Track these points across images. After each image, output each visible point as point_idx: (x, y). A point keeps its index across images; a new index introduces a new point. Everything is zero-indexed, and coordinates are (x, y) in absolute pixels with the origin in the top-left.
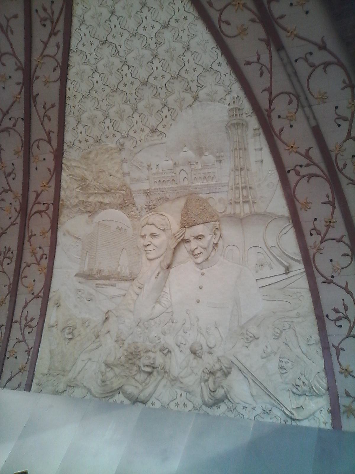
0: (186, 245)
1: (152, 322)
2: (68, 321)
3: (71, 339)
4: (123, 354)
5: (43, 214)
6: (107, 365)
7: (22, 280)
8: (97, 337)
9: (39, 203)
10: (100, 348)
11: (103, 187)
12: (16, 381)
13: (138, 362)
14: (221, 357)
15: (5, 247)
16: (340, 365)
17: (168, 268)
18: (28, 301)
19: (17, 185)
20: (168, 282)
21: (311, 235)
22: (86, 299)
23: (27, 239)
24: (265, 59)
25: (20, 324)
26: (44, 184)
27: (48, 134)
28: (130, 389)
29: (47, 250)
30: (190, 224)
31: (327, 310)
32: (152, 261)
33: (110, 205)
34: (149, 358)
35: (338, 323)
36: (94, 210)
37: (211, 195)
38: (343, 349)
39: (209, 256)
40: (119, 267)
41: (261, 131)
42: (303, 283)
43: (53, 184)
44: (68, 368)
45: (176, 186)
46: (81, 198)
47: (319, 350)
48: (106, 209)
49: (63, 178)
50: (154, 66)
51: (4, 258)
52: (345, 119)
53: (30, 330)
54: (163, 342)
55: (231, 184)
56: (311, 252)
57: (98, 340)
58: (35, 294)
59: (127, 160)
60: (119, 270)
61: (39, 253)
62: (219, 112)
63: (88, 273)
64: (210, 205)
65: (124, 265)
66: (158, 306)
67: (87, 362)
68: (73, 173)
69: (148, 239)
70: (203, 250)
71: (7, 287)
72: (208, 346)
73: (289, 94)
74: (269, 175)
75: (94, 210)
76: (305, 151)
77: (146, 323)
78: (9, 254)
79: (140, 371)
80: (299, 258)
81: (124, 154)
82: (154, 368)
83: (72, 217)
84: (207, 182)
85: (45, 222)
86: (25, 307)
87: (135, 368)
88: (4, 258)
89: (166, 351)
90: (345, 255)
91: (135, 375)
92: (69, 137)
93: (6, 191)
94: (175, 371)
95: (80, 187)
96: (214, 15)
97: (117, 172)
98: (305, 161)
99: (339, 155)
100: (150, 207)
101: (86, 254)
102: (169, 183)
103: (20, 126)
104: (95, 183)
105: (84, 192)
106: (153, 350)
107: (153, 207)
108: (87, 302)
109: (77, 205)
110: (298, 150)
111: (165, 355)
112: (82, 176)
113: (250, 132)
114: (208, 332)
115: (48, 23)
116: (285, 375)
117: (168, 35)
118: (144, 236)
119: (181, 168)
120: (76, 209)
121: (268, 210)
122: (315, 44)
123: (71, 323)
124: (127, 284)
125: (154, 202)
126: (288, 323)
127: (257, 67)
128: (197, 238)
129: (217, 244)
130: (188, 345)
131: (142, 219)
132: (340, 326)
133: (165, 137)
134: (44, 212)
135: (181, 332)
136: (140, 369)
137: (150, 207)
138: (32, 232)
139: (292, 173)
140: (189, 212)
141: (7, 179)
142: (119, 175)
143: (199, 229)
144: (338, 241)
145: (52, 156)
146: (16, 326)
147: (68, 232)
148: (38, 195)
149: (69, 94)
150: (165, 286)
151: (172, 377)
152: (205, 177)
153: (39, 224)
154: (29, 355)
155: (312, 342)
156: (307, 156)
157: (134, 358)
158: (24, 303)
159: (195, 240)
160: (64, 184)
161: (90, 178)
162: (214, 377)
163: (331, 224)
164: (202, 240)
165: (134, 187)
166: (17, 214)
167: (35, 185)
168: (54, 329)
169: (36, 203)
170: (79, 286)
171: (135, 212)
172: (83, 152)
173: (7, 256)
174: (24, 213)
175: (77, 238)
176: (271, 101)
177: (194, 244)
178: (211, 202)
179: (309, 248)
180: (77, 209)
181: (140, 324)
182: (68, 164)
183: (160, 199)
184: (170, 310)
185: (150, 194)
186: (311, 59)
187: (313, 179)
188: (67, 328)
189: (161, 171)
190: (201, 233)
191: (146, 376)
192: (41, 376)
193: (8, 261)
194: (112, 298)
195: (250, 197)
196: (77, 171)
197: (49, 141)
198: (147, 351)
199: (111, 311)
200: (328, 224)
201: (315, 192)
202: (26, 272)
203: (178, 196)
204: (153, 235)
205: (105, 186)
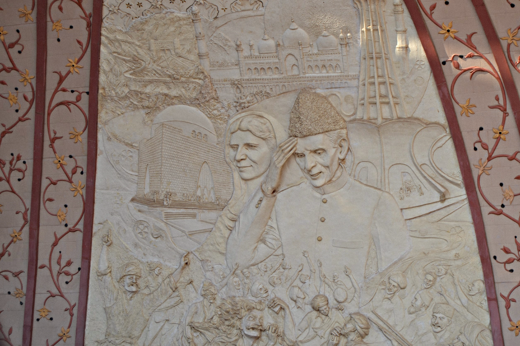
0: (298, 159)
1: (254, 269)
2: (127, 265)
3: (134, 292)
4: (216, 313)
5: (72, 106)
7: (44, 204)
9: (64, 90)
10: (181, 306)
11: (168, 73)
13: (238, 323)
14: (356, 314)
15: (12, 154)
16: (510, 320)
17: (274, 192)
18: (58, 236)
19: (27, 62)
20: (273, 213)
21: (475, 149)
22: (152, 235)
25: (50, 270)
26: (71, 62)
29: (83, 162)
30: (305, 133)
31: (494, 250)
32: (249, 182)
33: (180, 99)
34: (255, 318)
35: (509, 267)
36: (155, 105)
37: (334, 91)
38: (514, 301)
39: (334, 176)
40: (199, 189)
41: (404, 6)
44: (136, 333)
45: (281, 76)
46: (133, 88)
47: (483, 302)
48: (173, 104)
49: (102, 56)
51: (11, 170)
53: (68, 278)
54: (272, 296)
55: (361, 78)
56: (475, 172)
57: (177, 293)
58: (69, 226)
59: (204, 36)
60: (199, 193)
61: (70, 165)
63: (152, 197)
64: (332, 106)
66: (262, 246)
67: (164, 325)
68: (119, 50)
69: (242, 152)
70: (323, 168)
71: (20, 215)
72: (336, 300)
74: (417, 67)
75: (155, 105)
76: (466, 37)
77: (245, 270)
78: (20, 165)
79: (242, 335)
80: (459, 179)
81: (200, 27)
82: (261, 330)
83: (120, 113)
84: (328, 72)
86: (55, 244)
88: (11, 170)
89: (277, 307)
91: (237, 340)
93: (8, 70)
94: (291, 335)
95: (130, 70)
97: (189, 52)
99: (512, 47)
100: (243, 105)
101: (146, 168)
102: (269, 73)
104: (155, 66)
105: (138, 79)
106: (258, 308)
107: (246, 105)
108: (154, 239)
109: (126, 97)
110: (456, 35)
111: (277, 313)
112: (135, 56)
114: (336, 281)
116: (439, 335)
118: (235, 147)
119: (290, 51)
120: (127, 102)
121: (415, 115)
123: (132, 269)
124: (212, 215)
125: (248, 98)
126: (444, 267)
128: (315, 152)
129: (343, 160)
130: (308, 300)
131: (231, 121)
132: (512, 271)
133: (263, 6)
135: (297, 282)
136: (243, 333)
137: (243, 105)
138: (55, 133)
140: (302, 117)
141: (8, 53)
142: (193, 57)
143: (318, 141)
144: (511, 159)
145: (84, 23)
147: (115, 137)
148: (62, 80)
150: (270, 218)
151: (288, 342)
152: (324, 66)
153: (66, 122)
154: (72, 315)
155: (475, 291)
157: (233, 318)
158: (53, 240)
159: (312, 154)
160: (104, 65)
161: (147, 58)
162: (345, 340)
163: (502, 136)
164: (323, 155)
165: (216, 75)
166: (28, 105)
167: (55, 63)
168: (108, 278)
169: (59, 89)
170: (140, 217)
171: (218, 111)
172: (134, 20)
173: (16, 167)
177: (310, 160)
179: (472, 167)
180: (128, 102)
181: (237, 272)
182: (111, 36)
183: (257, 94)
184: (279, 252)
185: (242, 86)
188: (129, 277)
189: (257, 54)
190: (321, 147)
191: (251, 343)
192: (96, 344)
193: (20, 175)
194: (191, 234)
195: (390, 97)
196: (126, 47)
198: (250, 309)
199: (192, 253)
200: (498, 135)
202: (51, 192)
203: (284, 90)
204: (249, 146)
205: (171, 71)
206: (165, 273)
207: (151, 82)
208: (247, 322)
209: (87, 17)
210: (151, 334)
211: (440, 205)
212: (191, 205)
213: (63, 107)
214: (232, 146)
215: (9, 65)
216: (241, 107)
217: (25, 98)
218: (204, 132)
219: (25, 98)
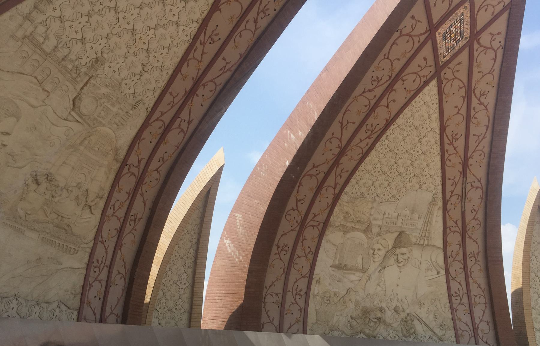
3: (328, 304)
5: (315, 228)
6: (352, 318)
8: (345, 303)
9: (314, 221)
12: (294, 328)
19: (303, 208)
23: (301, 240)
24: (456, 180)
25: (292, 292)
27: (336, 185)
28: (367, 331)
31: (453, 293)
33: (358, 230)
42: (443, 279)
43: (327, 211)
46: (342, 223)
50: (409, 169)
52: (475, 210)
60: (357, 266)
61: (308, 250)
62: (428, 197)
65: (359, 262)
66: (379, 288)
73: (458, 195)
80: (444, 267)
81: (375, 205)
85: (316, 233)
86: (295, 283)
87: (367, 320)
88: (282, 250)
89: (381, 309)
90: (461, 268)
92: (347, 189)
93: (293, 210)
94: (388, 320)
96: (446, 155)
97: (368, 213)
98: (455, 225)
103: (321, 176)
113: (437, 207)
115: (369, 132)
117: (423, 157)
122: (477, 179)
124: (362, 274)
127: (452, 181)
131: (374, 240)
134: (316, 226)
135: (389, 301)
139: (448, 229)
142: (368, 215)
143: (404, 250)
146: (289, 295)
147: (330, 241)
148: (315, 216)
149: (360, 169)
153: (310, 233)
154: (301, 312)
156: (456, 223)
160: (334, 213)
161: (352, 213)
174: (303, 225)
175: (335, 245)
176: (451, 197)
178: (410, 236)
182: (341, 203)
184: (384, 289)
186: (473, 184)
187: (456, 233)
193: (285, 253)
194: (352, 281)
196: (345, 208)
197: (334, 189)
198: (373, 311)
201: (455, 239)
202: (297, 261)
204: (379, 249)
206: (341, 296)
207: (350, 222)
208: (372, 316)
209: (334, 195)
210: (335, 321)
211: (437, 276)
212: (354, 269)
213: (312, 227)
214: (372, 249)
215: (295, 208)
216: (379, 234)
217: (297, 222)
218: (363, 243)
219: (297, 222)
